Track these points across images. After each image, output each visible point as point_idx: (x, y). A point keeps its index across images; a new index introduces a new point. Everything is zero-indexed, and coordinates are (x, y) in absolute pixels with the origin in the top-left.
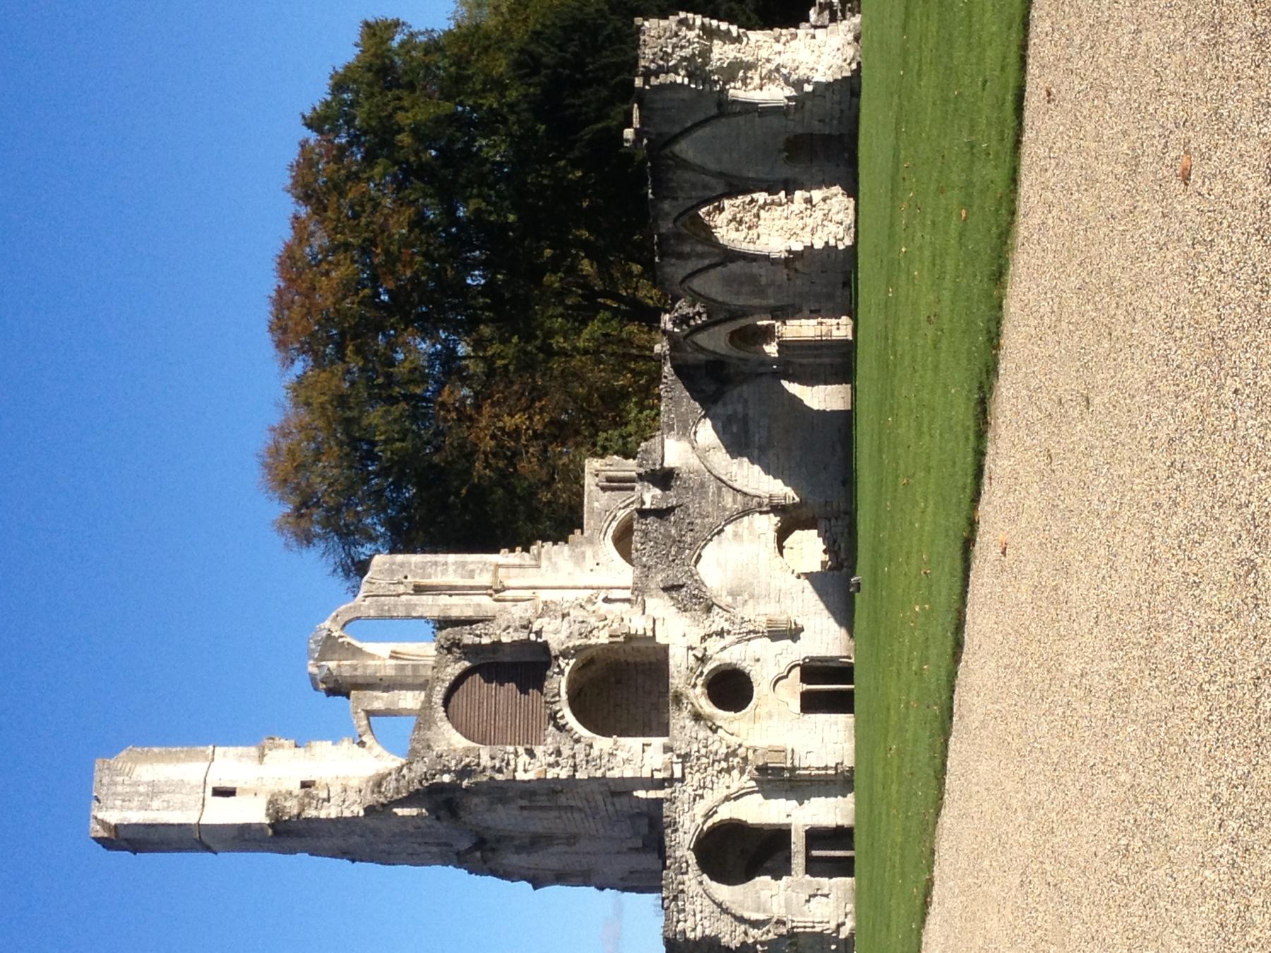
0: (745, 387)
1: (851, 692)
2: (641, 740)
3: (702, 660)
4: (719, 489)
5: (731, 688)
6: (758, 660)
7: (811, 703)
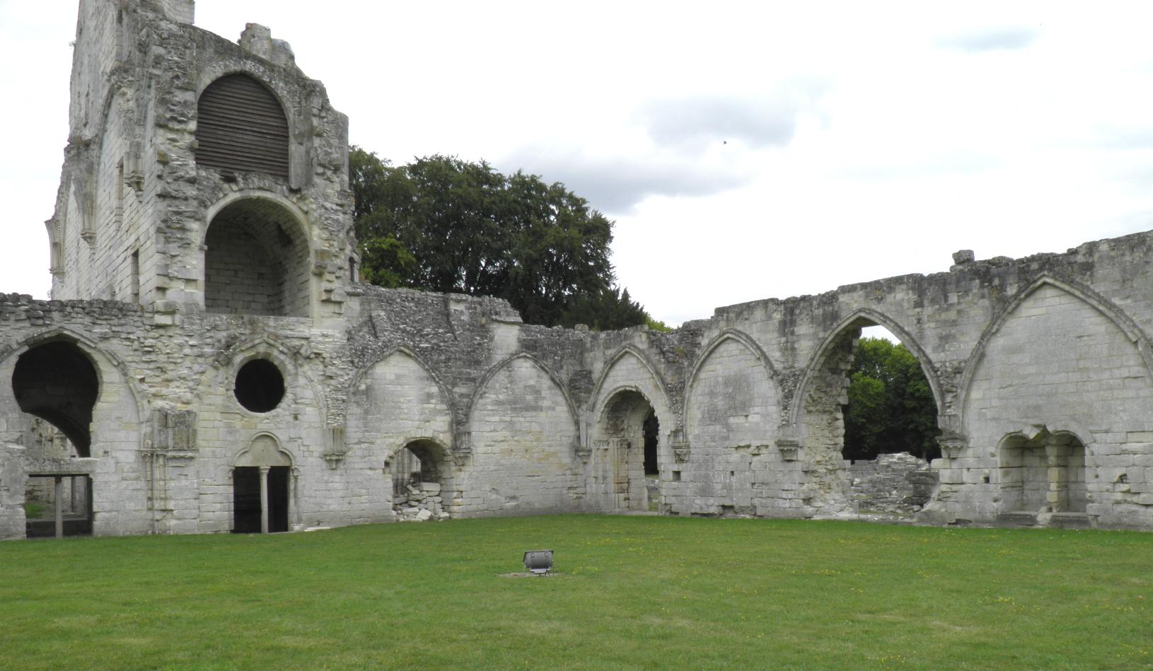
0: (565, 408)
1: (257, 529)
2: (201, 278)
3: (296, 354)
4: (474, 380)
5: (260, 386)
6: (296, 418)
7: (244, 479)
